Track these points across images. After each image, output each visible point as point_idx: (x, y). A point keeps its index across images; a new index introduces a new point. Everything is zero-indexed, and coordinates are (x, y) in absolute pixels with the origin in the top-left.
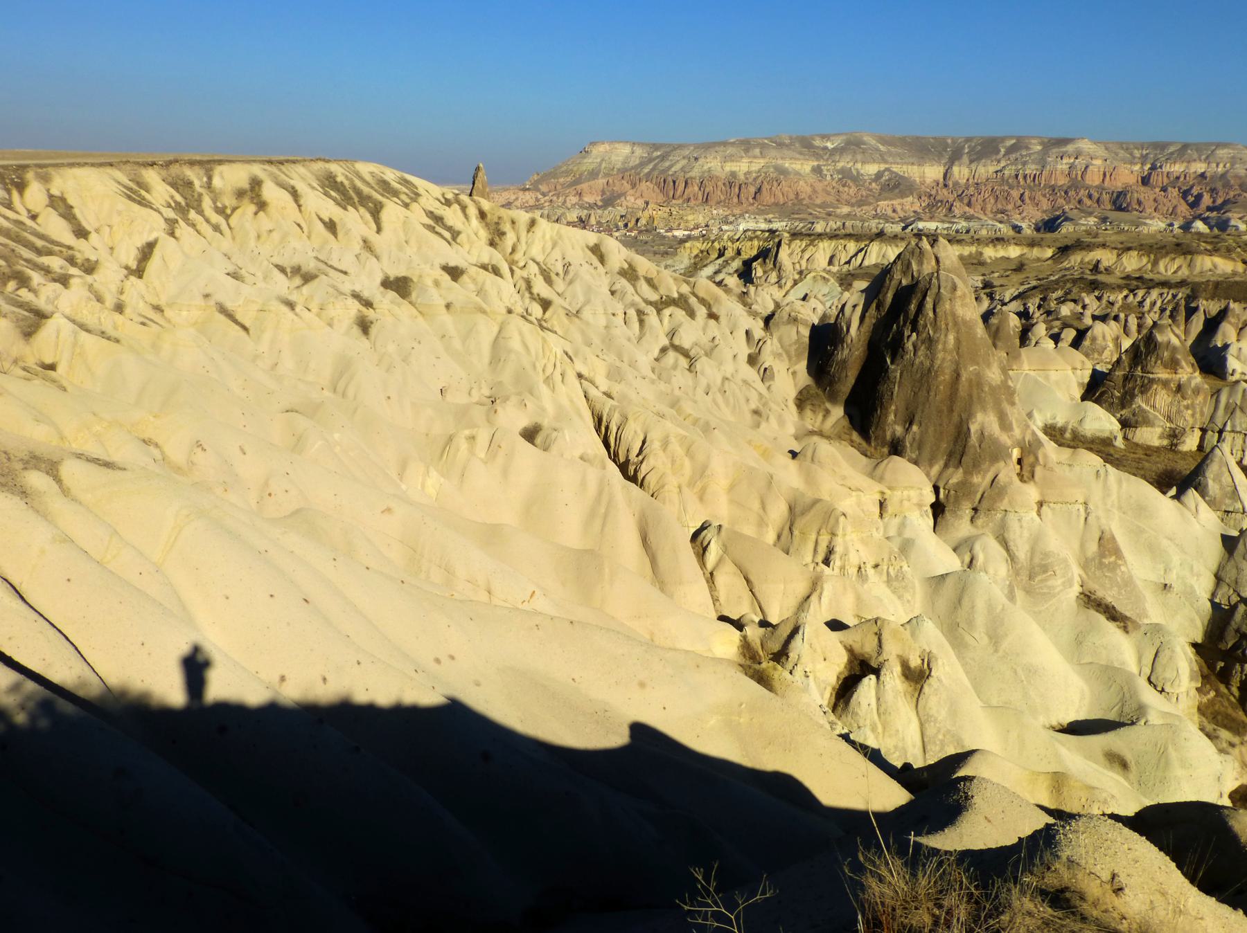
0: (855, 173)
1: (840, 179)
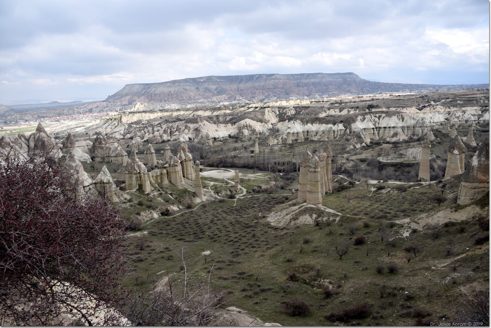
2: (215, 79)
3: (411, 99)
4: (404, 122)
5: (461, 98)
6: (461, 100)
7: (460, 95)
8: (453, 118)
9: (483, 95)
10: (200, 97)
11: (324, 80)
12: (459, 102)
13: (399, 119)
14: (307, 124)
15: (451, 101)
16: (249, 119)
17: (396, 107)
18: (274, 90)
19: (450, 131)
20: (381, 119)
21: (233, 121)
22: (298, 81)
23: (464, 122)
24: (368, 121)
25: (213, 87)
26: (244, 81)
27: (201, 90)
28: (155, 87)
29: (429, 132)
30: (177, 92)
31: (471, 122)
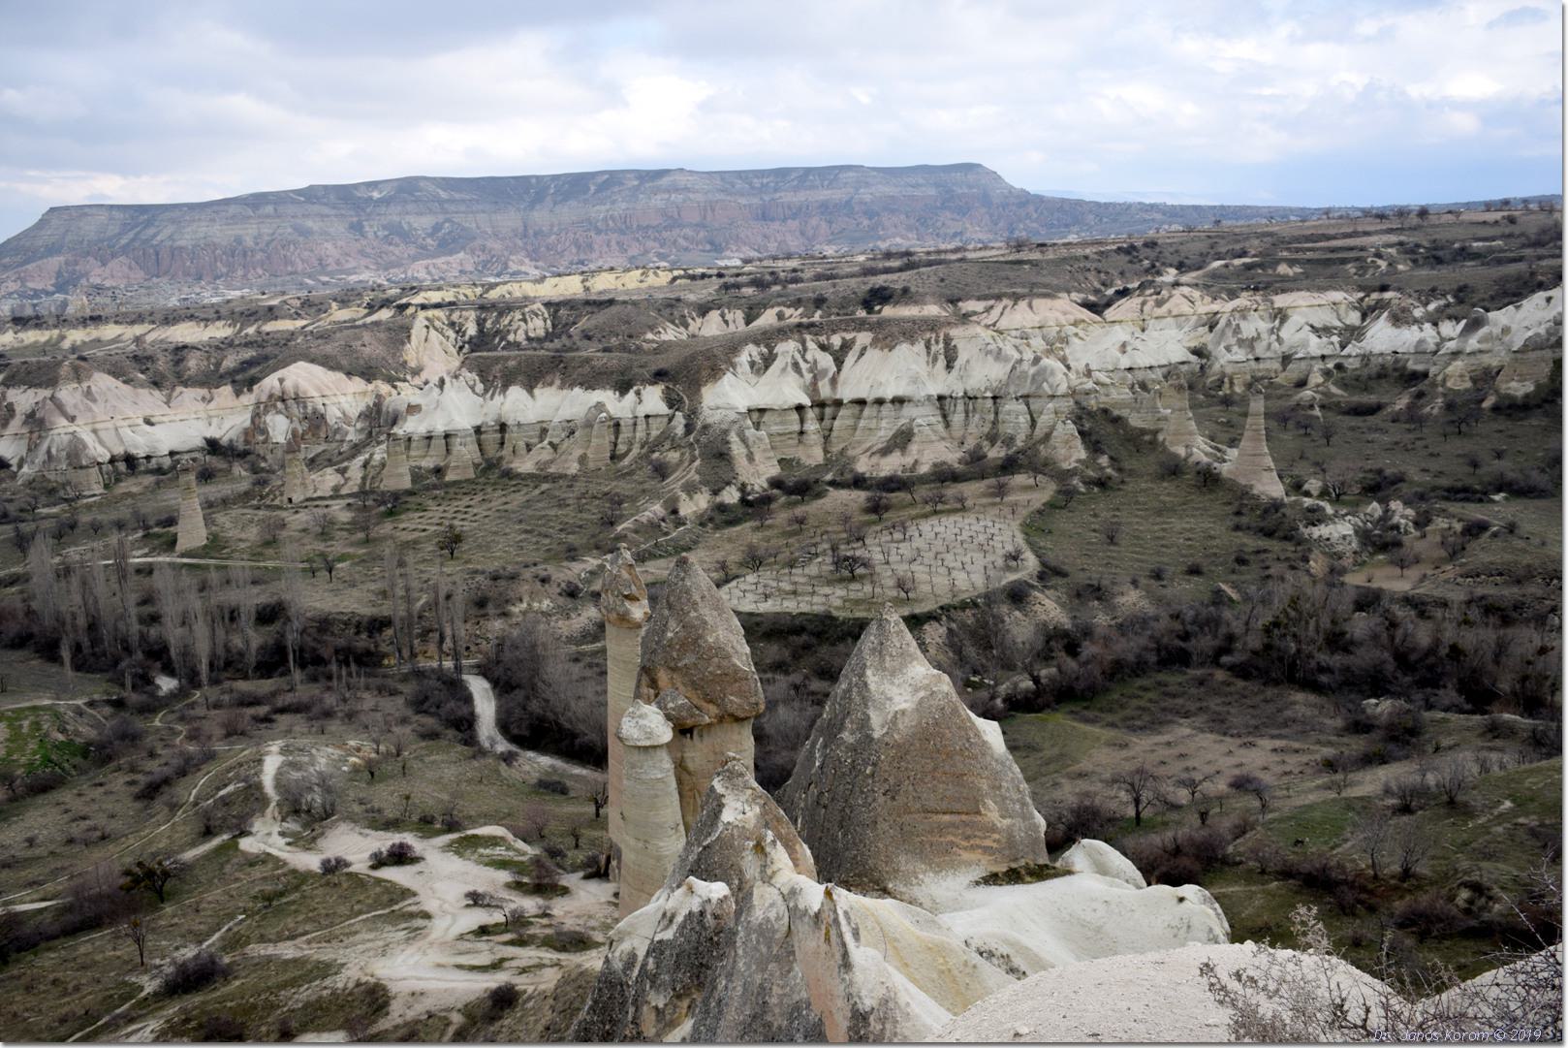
0: (406, 227)
1: (386, 236)
2: (431, 188)
3: (1076, 259)
4: (955, 372)
5: (1297, 250)
6: (1291, 263)
7: (1297, 240)
8: (1228, 349)
9: (1393, 238)
10: (364, 262)
11: (865, 195)
12: (1283, 269)
13: (935, 360)
14: (505, 387)
15: (1249, 267)
16: (312, 361)
17: (985, 298)
18: (665, 234)
19: (1165, 419)
20: (850, 359)
21: (244, 379)
22: (767, 198)
23: (1276, 365)
24: (784, 370)
25: (422, 223)
26: (549, 198)
27: (370, 235)
28: (173, 221)
29: (1060, 426)
30: (268, 244)
31: (1303, 365)
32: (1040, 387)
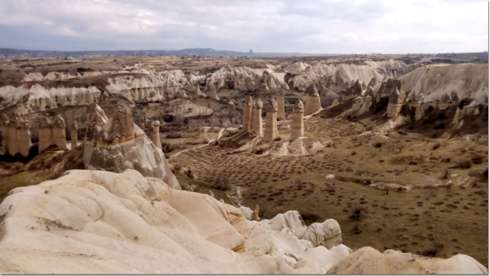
6: (151, 65)
32: (173, 85)
